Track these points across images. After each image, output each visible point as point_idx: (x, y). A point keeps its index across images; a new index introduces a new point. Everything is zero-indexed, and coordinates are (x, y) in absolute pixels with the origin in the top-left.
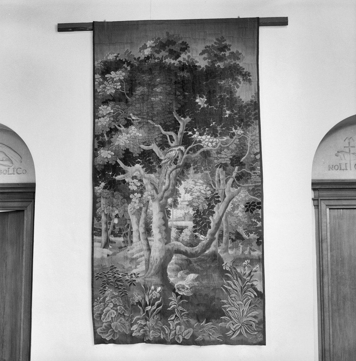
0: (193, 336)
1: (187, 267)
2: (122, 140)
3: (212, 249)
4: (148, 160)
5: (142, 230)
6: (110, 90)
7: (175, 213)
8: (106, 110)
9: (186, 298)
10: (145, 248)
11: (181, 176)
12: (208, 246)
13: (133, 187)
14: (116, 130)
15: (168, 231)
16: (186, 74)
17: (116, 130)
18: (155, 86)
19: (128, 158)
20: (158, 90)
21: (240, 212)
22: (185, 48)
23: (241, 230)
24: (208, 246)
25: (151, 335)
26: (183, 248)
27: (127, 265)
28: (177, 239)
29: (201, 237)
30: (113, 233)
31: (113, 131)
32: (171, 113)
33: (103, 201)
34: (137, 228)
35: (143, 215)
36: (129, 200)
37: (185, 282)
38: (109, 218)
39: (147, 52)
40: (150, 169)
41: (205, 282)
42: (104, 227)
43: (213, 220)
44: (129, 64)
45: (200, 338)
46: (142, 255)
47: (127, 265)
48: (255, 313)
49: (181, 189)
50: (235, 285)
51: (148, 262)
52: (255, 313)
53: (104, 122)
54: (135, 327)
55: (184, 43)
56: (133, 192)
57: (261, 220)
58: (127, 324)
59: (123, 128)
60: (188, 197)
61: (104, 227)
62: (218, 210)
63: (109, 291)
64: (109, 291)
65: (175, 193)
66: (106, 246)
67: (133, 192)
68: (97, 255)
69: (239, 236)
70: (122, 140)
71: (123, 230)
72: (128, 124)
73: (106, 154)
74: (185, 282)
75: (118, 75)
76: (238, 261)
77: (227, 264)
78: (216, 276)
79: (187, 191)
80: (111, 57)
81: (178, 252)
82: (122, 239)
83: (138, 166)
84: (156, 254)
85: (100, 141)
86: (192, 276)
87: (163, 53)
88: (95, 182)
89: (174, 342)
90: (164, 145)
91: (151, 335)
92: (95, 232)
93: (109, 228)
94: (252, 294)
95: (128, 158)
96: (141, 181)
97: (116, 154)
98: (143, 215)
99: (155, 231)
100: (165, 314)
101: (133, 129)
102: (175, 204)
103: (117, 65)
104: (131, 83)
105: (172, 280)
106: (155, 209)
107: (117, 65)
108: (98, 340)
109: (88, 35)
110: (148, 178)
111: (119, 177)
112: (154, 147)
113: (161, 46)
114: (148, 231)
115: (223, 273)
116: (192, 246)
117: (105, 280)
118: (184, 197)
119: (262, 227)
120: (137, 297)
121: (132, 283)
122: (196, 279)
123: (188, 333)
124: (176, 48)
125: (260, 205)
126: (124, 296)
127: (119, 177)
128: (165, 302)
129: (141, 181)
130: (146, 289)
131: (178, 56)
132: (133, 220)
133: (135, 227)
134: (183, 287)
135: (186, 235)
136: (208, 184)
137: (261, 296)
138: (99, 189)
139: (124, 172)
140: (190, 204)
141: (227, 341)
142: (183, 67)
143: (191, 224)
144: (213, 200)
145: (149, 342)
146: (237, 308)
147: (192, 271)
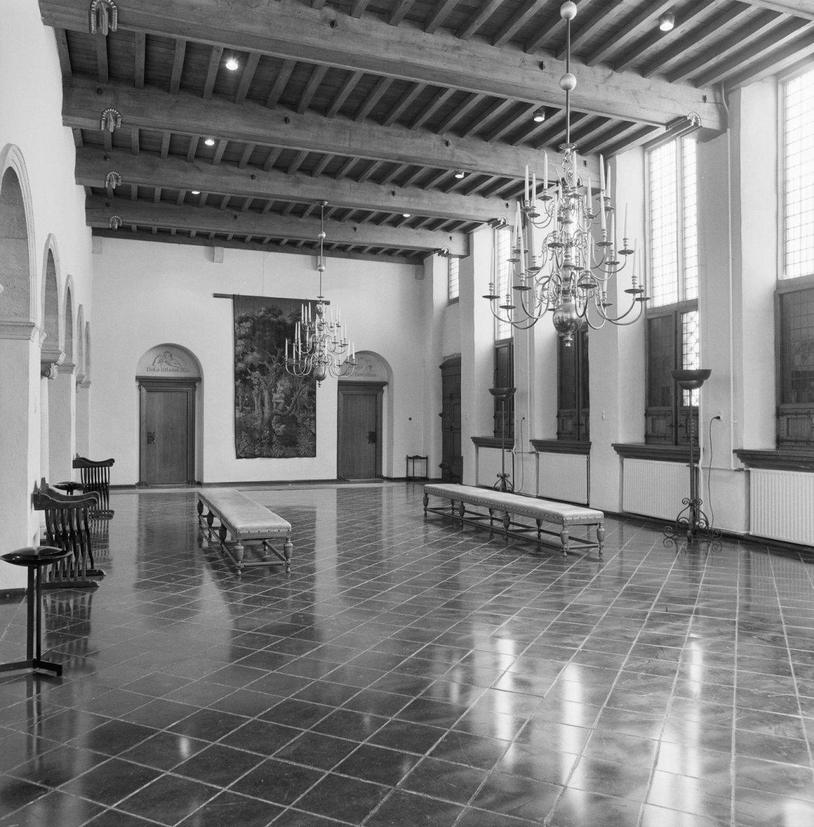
0: (284, 454)
1: (280, 422)
2: (249, 358)
3: (293, 413)
4: (263, 370)
5: (259, 404)
6: (243, 333)
7: (275, 396)
8: (240, 342)
9: (280, 436)
10: (261, 412)
11: (278, 377)
12: (290, 412)
13: (255, 383)
14: (247, 353)
15: (272, 404)
16: (282, 327)
17: (247, 353)
18: (266, 332)
19: (253, 368)
20: (267, 334)
21: (305, 396)
22: (281, 313)
23: (306, 405)
24: (290, 412)
25: (265, 454)
26: (279, 413)
27: (252, 420)
28: (276, 408)
29: (288, 407)
30: (245, 405)
31: (244, 354)
32: (273, 346)
33: (240, 389)
34: (257, 403)
35: (260, 397)
36: (253, 389)
37: (280, 429)
38: (243, 397)
39: (261, 313)
40: (263, 374)
41: (289, 429)
42: (240, 402)
43: (293, 399)
44: (253, 319)
45: (287, 454)
46: (259, 416)
47: (252, 420)
48: (311, 443)
49: (278, 385)
50: (303, 430)
51: (262, 419)
52: (311, 443)
53: (240, 349)
54: (256, 450)
55: (280, 310)
56: (255, 385)
57: (315, 400)
58: (252, 449)
59: (249, 352)
60: (282, 388)
61: (240, 402)
62: (295, 395)
63: (243, 433)
64: (243, 433)
65: (276, 386)
66: (242, 411)
67: (255, 385)
68: (237, 416)
69: (305, 407)
70: (249, 358)
71: (250, 403)
72: (253, 350)
73: (241, 365)
74: (280, 429)
75: (248, 324)
76: (304, 419)
77: (299, 420)
78: (294, 425)
79: (281, 385)
80: (243, 315)
81: (276, 414)
82: (249, 408)
83: (257, 372)
84: (266, 415)
85: (238, 358)
86: (283, 426)
87: (270, 315)
88: (236, 379)
89: (275, 457)
90: (270, 362)
91: (265, 454)
92: (236, 404)
93: (243, 401)
94: (311, 434)
95: (253, 368)
96: (259, 379)
97: (247, 365)
98: (260, 397)
99: (266, 404)
100: (270, 444)
101: (255, 354)
102: (275, 391)
103: (246, 319)
104: (253, 329)
105: (274, 428)
106: (266, 394)
107: (246, 319)
108: (238, 457)
109: (230, 301)
110: (262, 378)
111: (248, 377)
112: (265, 363)
113: (269, 311)
114: (263, 404)
115: (298, 425)
116: (283, 412)
117: (241, 428)
118: (280, 388)
119: (315, 404)
120: (257, 436)
121: (255, 429)
122: (285, 428)
123: (281, 453)
124: (276, 313)
125: (314, 393)
126: (251, 437)
127: (248, 377)
128: (271, 439)
129: (259, 379)
130: (261, 432)
131: (277, 317)
132: (255, 399)
133: (256, 403)
134: (279, 431)
135: (281, 406)
136: (291, 382)
137: (314, 435)
138: (238, 383)
139: (250, 375)
140: (283, 392)
141: (299, 456)
142: (280, 323)
143: (283, 401)
144: (293, 390)
145: (264, 457)
146: (304, 441)
147: (283, 423)
